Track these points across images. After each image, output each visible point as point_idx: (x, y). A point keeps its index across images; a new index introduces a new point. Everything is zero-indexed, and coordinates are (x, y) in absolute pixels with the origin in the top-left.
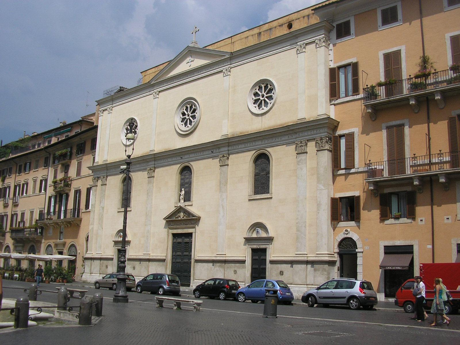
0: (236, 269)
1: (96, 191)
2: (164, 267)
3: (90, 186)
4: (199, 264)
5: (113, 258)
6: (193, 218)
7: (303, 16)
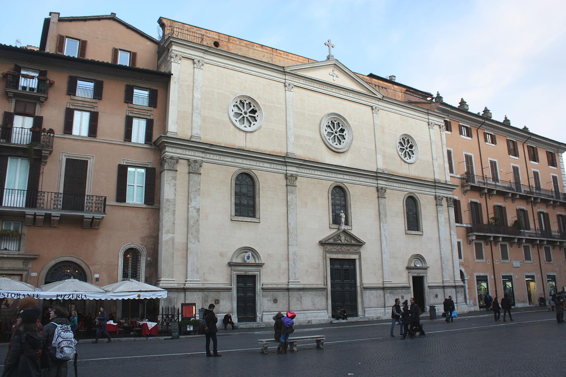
1: (175, 178)
3: (126, 163)
4: (367, 291)
5: (231, 289)
6: (360, 244)
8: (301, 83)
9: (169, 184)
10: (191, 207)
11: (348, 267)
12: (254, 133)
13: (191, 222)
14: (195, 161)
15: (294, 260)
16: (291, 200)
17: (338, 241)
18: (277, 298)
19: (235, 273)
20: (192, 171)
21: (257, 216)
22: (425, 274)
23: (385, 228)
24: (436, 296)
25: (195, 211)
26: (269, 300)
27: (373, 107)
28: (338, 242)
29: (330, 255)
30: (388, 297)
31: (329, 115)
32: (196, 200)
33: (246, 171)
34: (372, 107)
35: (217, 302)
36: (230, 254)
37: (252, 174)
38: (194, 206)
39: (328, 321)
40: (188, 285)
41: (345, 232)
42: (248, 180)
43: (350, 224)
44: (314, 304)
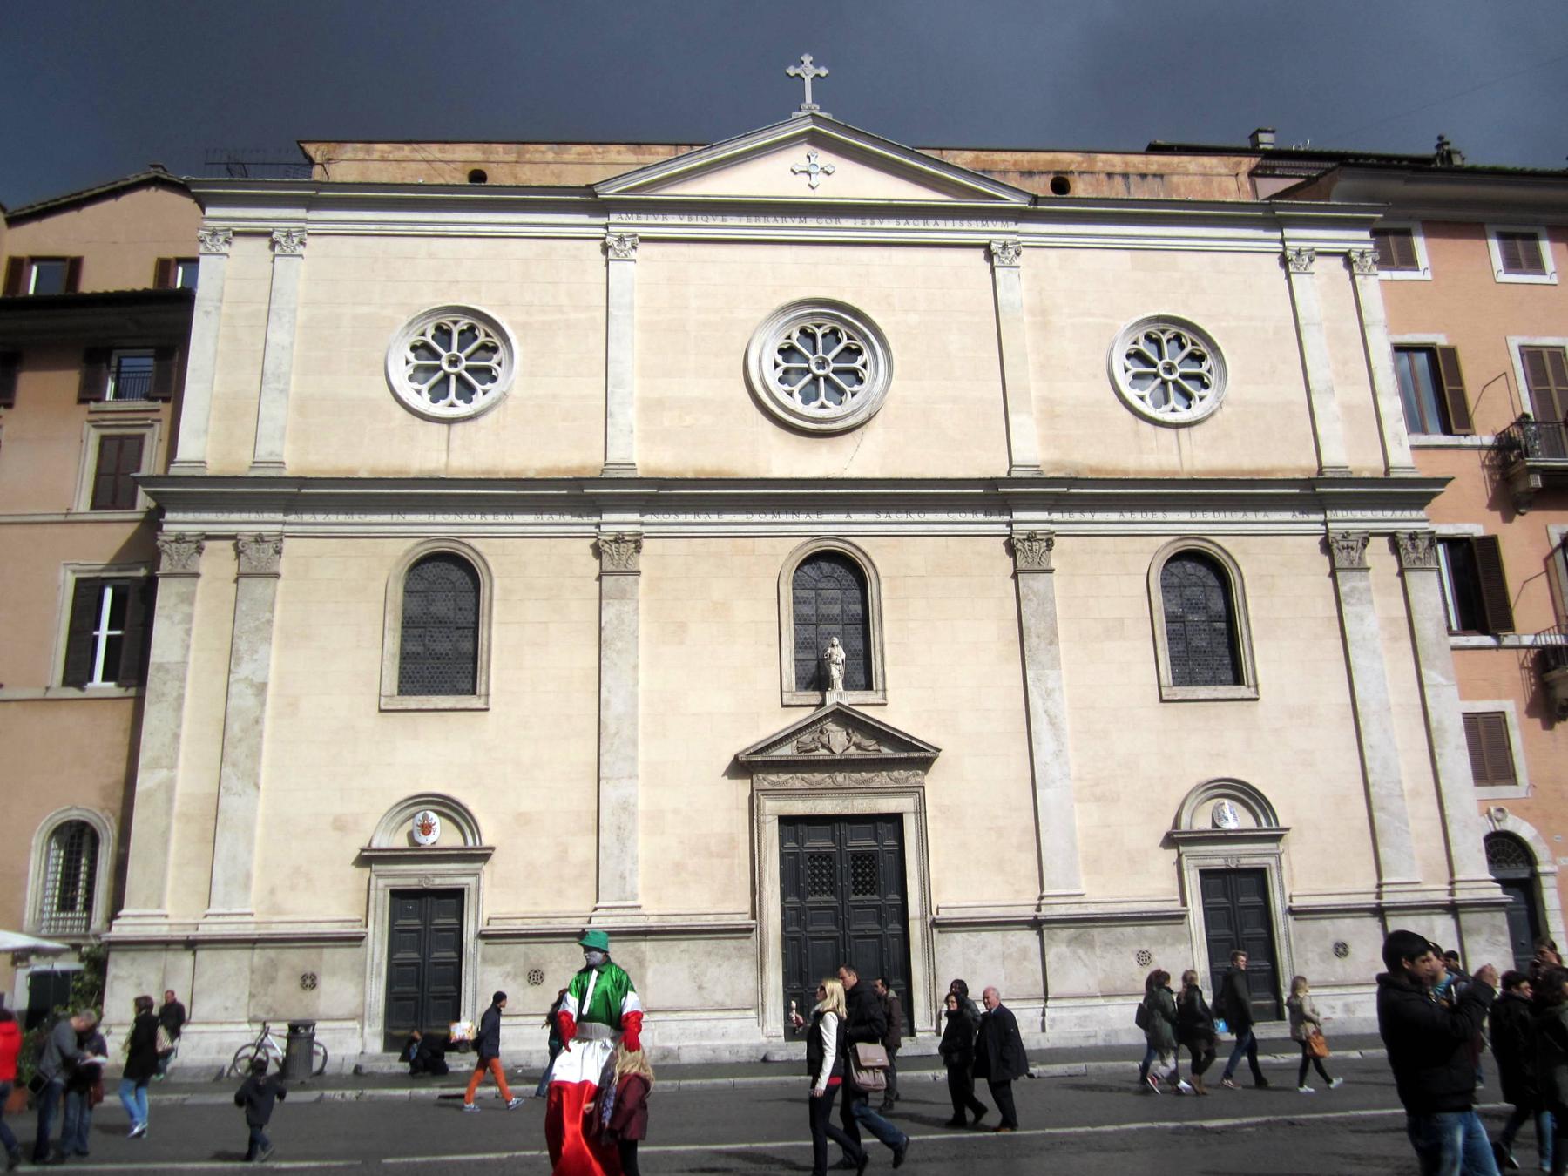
0: (1145, 948)
1: (189, 599)
2: (747, 961)
7: (1109, 169)
8: (674, 224)
9: (169, 617)
10: (238, 681)
11: (873, 843)
12: (482, 421)
13: (235, 728)
14: (259, 539)
15: (620, 828)
16: (616, 622)
17: (817, 749)
18: (543, 968)
19: (382, 882)
20: (248, 571)
21: (481, 688)
22: (1272, 861)
23: (1050, 685)
24: (1341, 950)
25: (249, 691)
26: (508, 974)
27: (993, 247)
28: (816, 753)
29: (782, 803)
30: (1060, 958)
31: (785, 309)
32: (255, 657)
33: (445, 547)
34: (986, 247)
35: (308, 982)
36: (370, 823)
37: (465, 552)
38: (246, 678)
39: (754, 1054)
40: (207, 927)
41: (844, 717)
42: (457, 574)
43: (877, 681)
44: (700, 987)
